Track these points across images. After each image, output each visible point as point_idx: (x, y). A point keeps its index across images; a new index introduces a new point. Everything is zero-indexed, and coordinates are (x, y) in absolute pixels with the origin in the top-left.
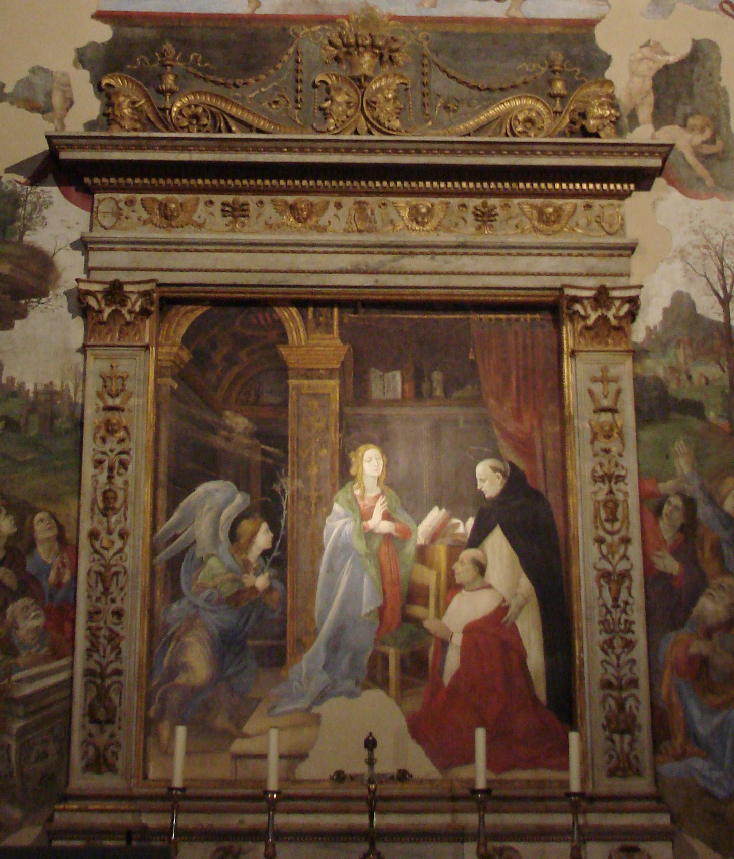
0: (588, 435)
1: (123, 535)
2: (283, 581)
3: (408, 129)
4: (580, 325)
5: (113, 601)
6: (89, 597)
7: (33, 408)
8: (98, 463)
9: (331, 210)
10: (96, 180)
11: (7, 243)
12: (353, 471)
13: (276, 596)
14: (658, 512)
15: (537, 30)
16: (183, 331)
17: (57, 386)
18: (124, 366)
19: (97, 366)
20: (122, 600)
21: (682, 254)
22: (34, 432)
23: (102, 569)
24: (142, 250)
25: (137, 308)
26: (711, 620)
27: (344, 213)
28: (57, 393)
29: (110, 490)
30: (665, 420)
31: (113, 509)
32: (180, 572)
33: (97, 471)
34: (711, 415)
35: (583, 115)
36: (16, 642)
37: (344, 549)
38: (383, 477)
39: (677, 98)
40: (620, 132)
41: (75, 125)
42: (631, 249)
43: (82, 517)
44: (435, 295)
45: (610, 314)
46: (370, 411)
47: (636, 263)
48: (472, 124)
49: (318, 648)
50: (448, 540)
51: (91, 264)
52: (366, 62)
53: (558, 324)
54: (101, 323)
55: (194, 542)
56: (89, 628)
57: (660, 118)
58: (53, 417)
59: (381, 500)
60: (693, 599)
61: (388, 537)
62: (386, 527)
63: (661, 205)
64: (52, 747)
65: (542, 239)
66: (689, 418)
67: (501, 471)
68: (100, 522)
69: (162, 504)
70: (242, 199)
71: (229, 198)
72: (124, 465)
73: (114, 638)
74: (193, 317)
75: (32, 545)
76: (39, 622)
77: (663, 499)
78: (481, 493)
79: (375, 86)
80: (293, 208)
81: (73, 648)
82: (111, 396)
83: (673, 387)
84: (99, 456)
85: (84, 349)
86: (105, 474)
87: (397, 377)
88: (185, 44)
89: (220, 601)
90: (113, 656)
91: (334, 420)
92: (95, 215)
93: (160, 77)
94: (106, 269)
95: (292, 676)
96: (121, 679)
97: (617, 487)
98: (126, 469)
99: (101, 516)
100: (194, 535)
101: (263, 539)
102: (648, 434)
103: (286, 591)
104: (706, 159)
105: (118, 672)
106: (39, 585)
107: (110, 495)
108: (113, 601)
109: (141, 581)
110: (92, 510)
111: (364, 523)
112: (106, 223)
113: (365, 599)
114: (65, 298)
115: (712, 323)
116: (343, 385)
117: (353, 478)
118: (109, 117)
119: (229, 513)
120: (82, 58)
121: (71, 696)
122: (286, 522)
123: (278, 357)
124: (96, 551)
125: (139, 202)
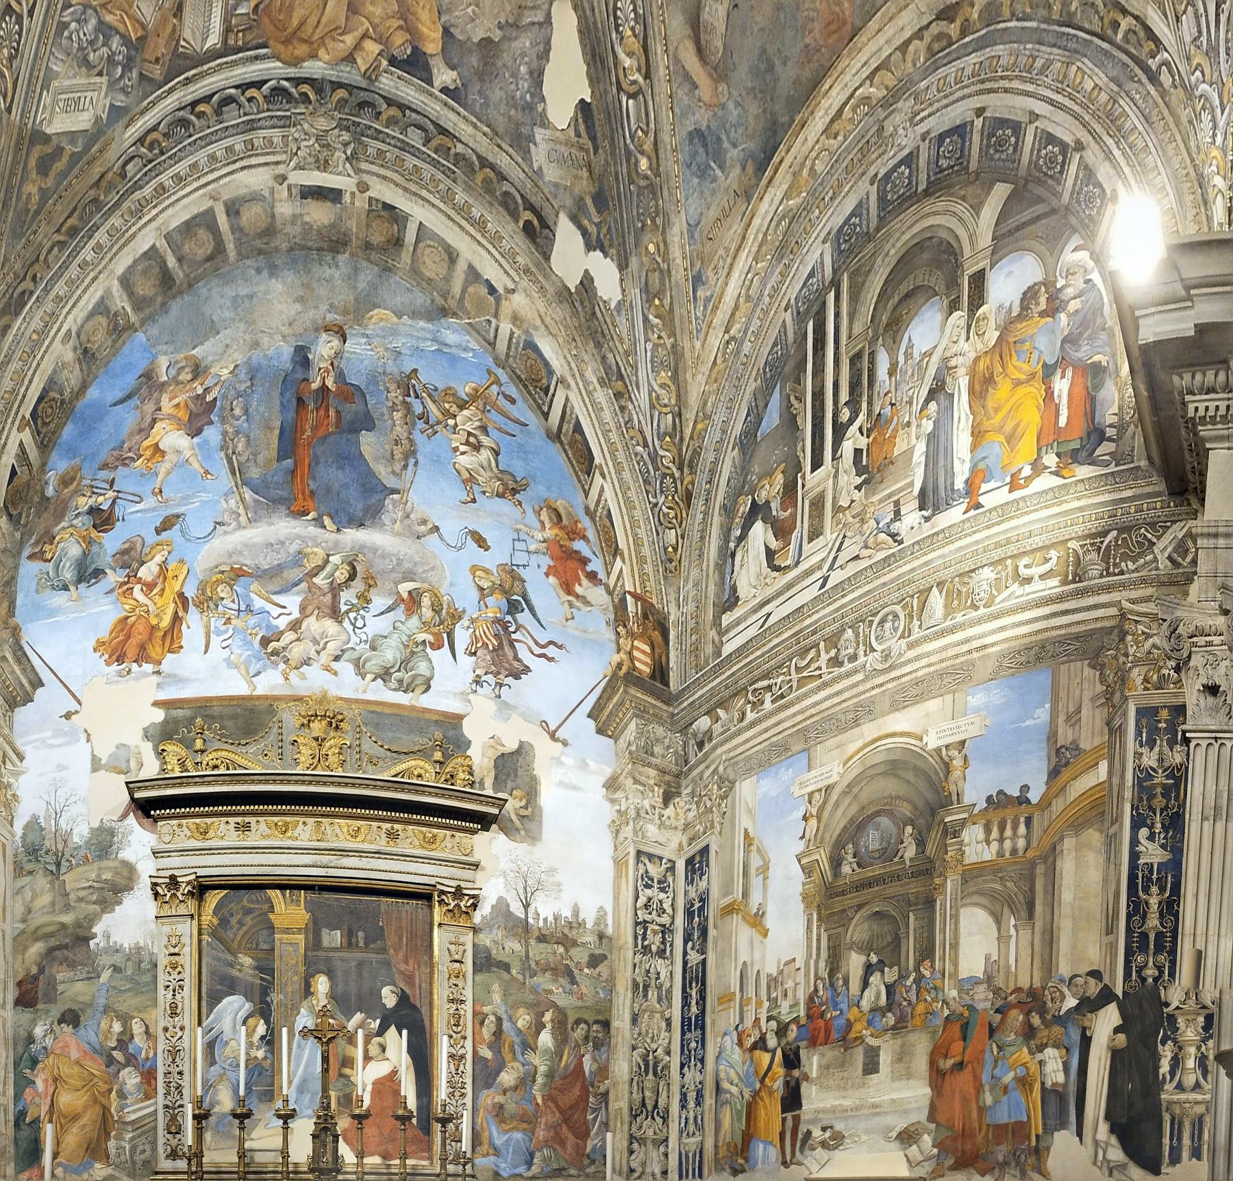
21: (504, 874)
26: (506, 1085)
34: (514, 972)
39: (508, 775)
63: (495, 842)
64: (148, 1147)
76: (138, 1079)
83: (494, 952)
105: (181, 1106)
106: (136, 1059)
115: (518, 918)
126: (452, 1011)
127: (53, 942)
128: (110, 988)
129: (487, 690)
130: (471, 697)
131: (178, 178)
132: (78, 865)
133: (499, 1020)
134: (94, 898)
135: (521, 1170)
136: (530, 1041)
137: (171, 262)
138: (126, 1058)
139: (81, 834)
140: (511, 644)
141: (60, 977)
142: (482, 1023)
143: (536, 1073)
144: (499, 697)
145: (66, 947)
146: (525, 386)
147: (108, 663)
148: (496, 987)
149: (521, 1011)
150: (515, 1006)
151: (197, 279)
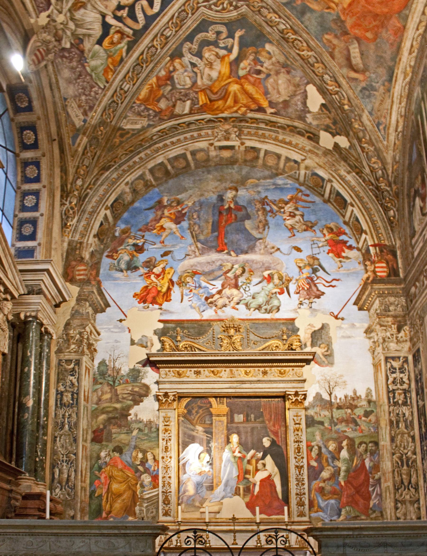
0: (292, 431)
1: (171, 457)
3: (244, 349)
4: (290, 401)
8: (163, 439)
9: (223, 372)
14: (311, 450)
15: (279, 321)
16: (184, 405)
17: (152, 420)
18: (169, 414)
19: (162, 414)
21: (319, 382)
22: (146, 431)
27: (226, 372)
30: (313, 426)
34: (326, 425)
35: (292, 345)
39: (318, 339)
40: (302, 349)
41: (154, 350)
42: (304, 381)
44: (252, 394)
45: (299, 398)
46: (234, 425)
47: (306, 384)
48: (261, 348)
52: (232, 331)
53: (285, 401)
57: (313, 345)
58: (151, 428)
60: (321, 472)
61: (240, 458)
62: (239, 455)
63: (313, 369)
65: (280, 379)
70: (199, 369)
71: (196, 369)
72: (170, 440)
75: (147, 460)
77: (313, 446)
78: (264, 446)
79: (234, 338)
80: (213, 372)
85: (158, 410)
87: (241, 416)
88: (183, 328)
91: (225, 428)
93: (176, 337)
102: (309, 430)
104: (325, 356)
116: (227, 418)
118: (163, 349)
120: (155, 333)
123: (210, 411)
128: (137, 438)
129: (305, 306)
130: (298, 310)
131: (173, 143)
132: (123, 383)
134: (130, 398)
135: (335, 518)
136: (337, 456)
137: (169, 167)
139: (125, 370)
140: (315, 285)
141: (113, 431)
143: (340, 470)
144: (311, 307)
145: (117, 418)
146: (313, 189)
147: (139, 303)
149: (331, 442)
150: (328, 440)
151: (179, 174)
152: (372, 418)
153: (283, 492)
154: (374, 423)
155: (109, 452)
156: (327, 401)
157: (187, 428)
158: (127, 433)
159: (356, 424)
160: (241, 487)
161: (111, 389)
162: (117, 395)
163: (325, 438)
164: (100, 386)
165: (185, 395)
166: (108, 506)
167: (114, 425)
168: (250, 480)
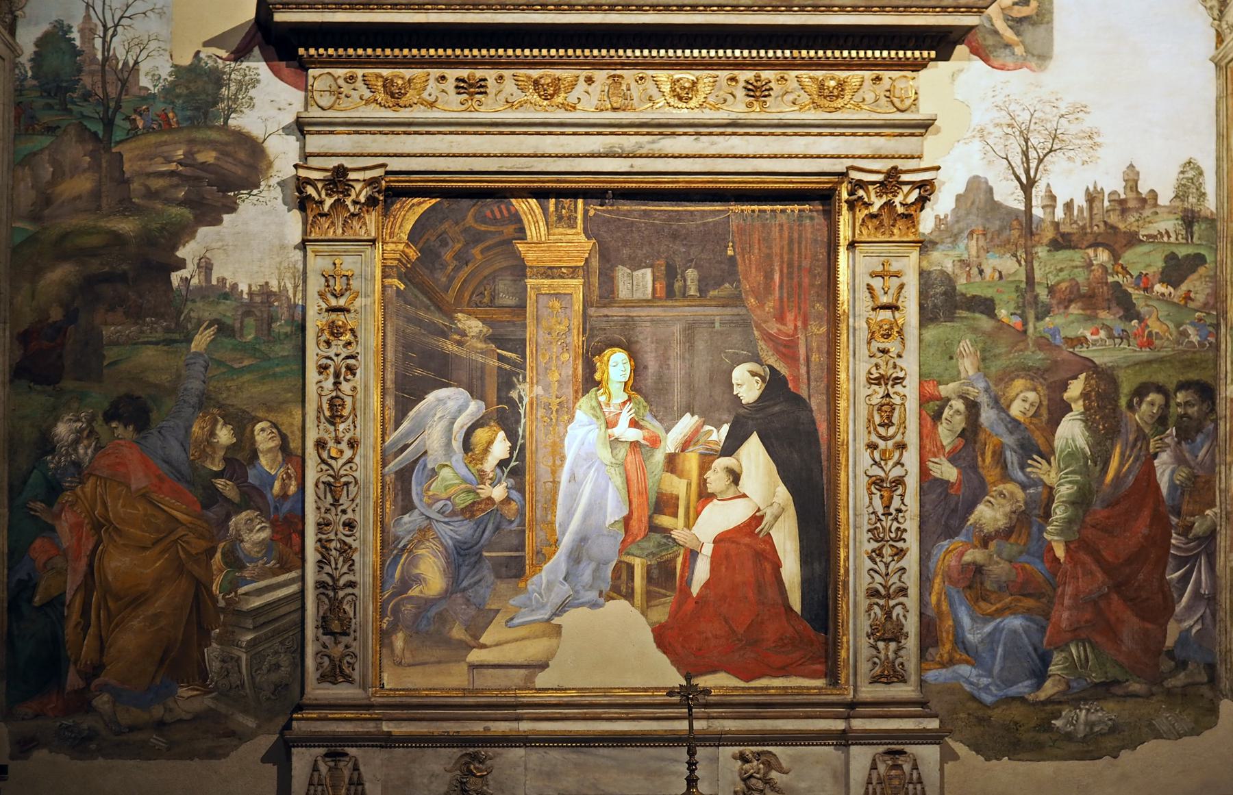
1: (353, 444)
2: (521, 490)
5: (344, 512)
6: (318, 508)
7: (248, 310)
8: (323, 369)
10: (312, 51)
11: (211, 128)
12: (597, 377)
13: (514, 506)
18: (349, 264)
19: (318, 263)
20: (354, 511)
23: (332, 480)
24: (367, 133)
25: (362, 199)
28: (274, 294)
29: (337, 397)
31: (341, 416)
32: (410, 483)
33: (321, 377)
34: (1002, 313)
36: (241, 555)
37: (590, 458)
38: (631, 382)
43: (308, 425)
46: (614, 312)
49: (558, 561)
50: (700, 449)
51: (308, 150)
54: (322, 215)
55: (426, 452)
56: (320, 540)
58: (272, 319)
59: (628, 406)
61: (635, 445)
62: (634, 435)
66: (977, 315)
67: (760, 376)
68: (327, 431)
69: (391, 413)
72: (351, 370)
73: (346, 550)
74: (426, 206)
75: (254, 455)
81: (303, 560)
82: (336, 297)
84: (324, 361)
85: (303, 245)
86: (331, 380)
89: (454, 513)
90: (345, 569)
91: (577, 322)
92: (310, 94)
94: (325, 155)
95: (529, 588)
96: (355, 591)
97: (894, 390)
98: (354, 374)
99: (327, 425)
100: (425, 446)
101: (500, 447)
103: (525, 499)
105: (352, 584)
106: (263, 496)
107: (338, 402)
108: (344, 512)
109: (374, 491)
110: (318, 418)
111: (610, 431)
112: (326, 101)
113: (609, 510)
114: (279, 189)
117: (598, 384)
119: (463, 421)
121: (303, 608)
122: (524, 431)
124: (323, 461)
125: (360, 78)
126: (876, 400)
127: (95, 266)
133: (973, 407)
138: (242, 494)
141: (108, 332)
142: (937, 416)
145: (123, 278)
148: (966, 345)
150: (1006, 377)
152: (1196, 285)
153: (806, 583)
154: (1205, 305)
155: (92, 419)
156: (1011, 212)
157: (419, 322)
158: (169, 342)
159: (1129, 311)
160: (639, 564)
161: (92, 154)
162: (125, 182)
163: (995, 367)
164: (45, 141)
165: (418, 182)
166: (89, 642)
167: (112, 309)
168: (675, 534)
